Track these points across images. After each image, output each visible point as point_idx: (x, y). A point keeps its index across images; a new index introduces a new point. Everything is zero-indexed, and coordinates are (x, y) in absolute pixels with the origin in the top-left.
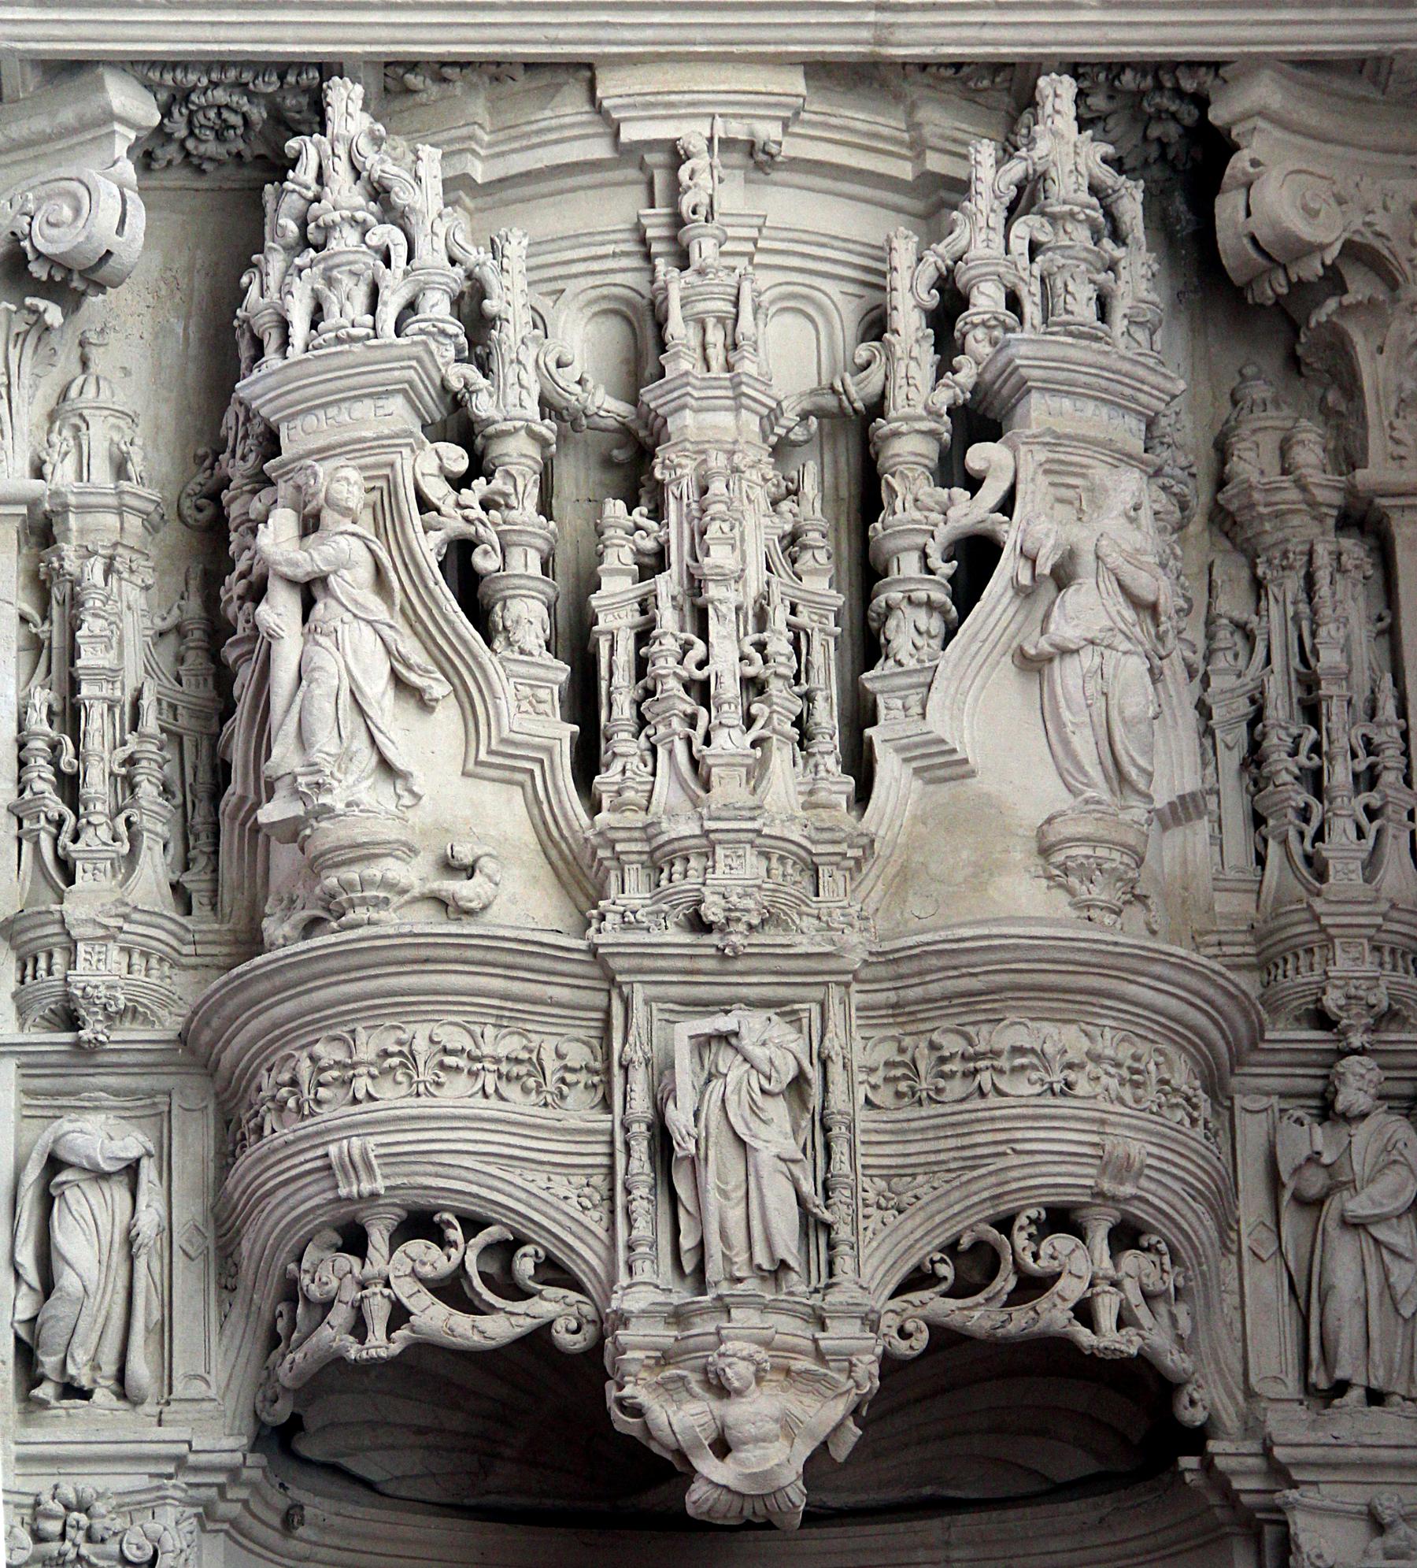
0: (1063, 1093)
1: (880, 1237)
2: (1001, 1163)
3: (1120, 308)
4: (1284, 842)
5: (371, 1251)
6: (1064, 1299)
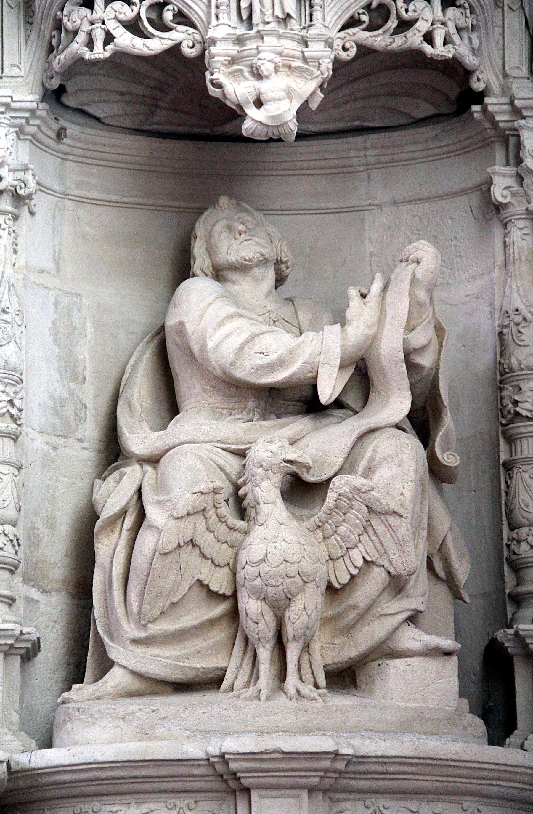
5: (96, 7)
6: (419, 31)
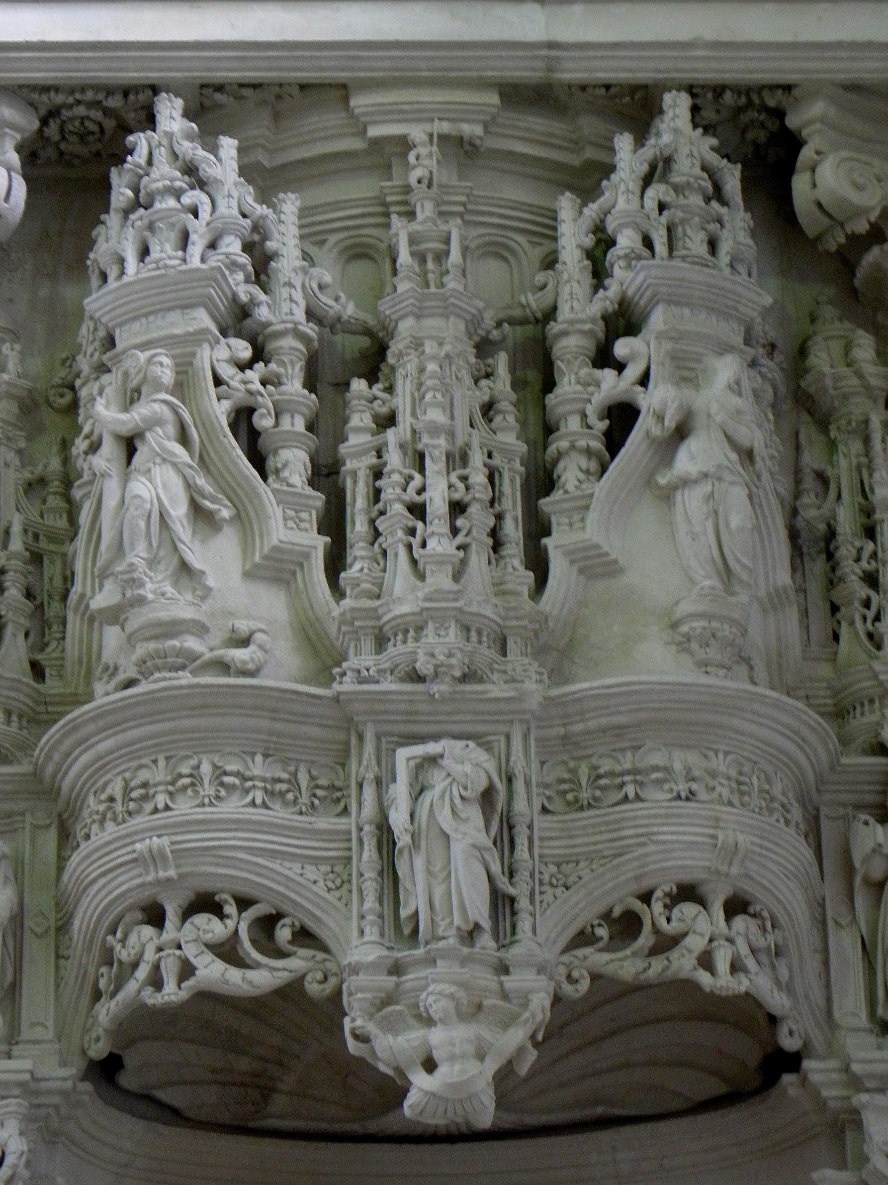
0: (688, 799)
1: (552, 907)
2: (641, 851)
3: (725, 247)
4: (852, 623)
5: (168, 924)
6: (690, 951)
